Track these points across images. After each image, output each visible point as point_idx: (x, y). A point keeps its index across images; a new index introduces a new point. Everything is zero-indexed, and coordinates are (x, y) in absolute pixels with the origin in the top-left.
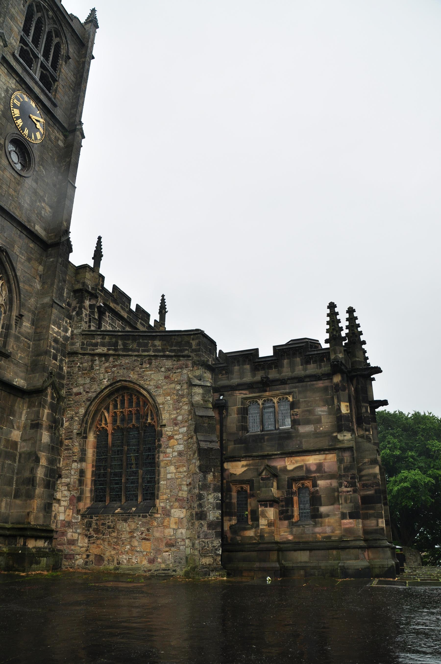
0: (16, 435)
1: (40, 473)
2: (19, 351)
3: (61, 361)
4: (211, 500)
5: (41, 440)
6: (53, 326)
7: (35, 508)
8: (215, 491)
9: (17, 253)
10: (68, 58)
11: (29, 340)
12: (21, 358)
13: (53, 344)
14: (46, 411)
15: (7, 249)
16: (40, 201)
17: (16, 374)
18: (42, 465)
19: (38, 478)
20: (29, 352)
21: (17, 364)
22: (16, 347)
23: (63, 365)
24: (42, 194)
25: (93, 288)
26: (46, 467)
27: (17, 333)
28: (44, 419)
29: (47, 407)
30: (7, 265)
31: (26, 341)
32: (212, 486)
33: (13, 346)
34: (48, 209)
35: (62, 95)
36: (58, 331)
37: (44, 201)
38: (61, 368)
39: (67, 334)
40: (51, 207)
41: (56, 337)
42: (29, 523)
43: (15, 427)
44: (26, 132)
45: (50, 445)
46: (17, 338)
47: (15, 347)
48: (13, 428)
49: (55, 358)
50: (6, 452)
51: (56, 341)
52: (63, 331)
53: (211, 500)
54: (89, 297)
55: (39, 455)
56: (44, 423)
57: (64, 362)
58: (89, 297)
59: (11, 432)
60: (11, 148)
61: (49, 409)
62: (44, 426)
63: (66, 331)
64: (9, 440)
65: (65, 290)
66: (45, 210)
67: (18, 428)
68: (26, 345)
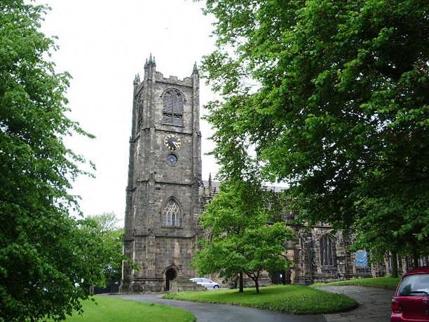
0: (190, 251)
10: (185, 101)
35: (187, 119)
60: (171, 156)
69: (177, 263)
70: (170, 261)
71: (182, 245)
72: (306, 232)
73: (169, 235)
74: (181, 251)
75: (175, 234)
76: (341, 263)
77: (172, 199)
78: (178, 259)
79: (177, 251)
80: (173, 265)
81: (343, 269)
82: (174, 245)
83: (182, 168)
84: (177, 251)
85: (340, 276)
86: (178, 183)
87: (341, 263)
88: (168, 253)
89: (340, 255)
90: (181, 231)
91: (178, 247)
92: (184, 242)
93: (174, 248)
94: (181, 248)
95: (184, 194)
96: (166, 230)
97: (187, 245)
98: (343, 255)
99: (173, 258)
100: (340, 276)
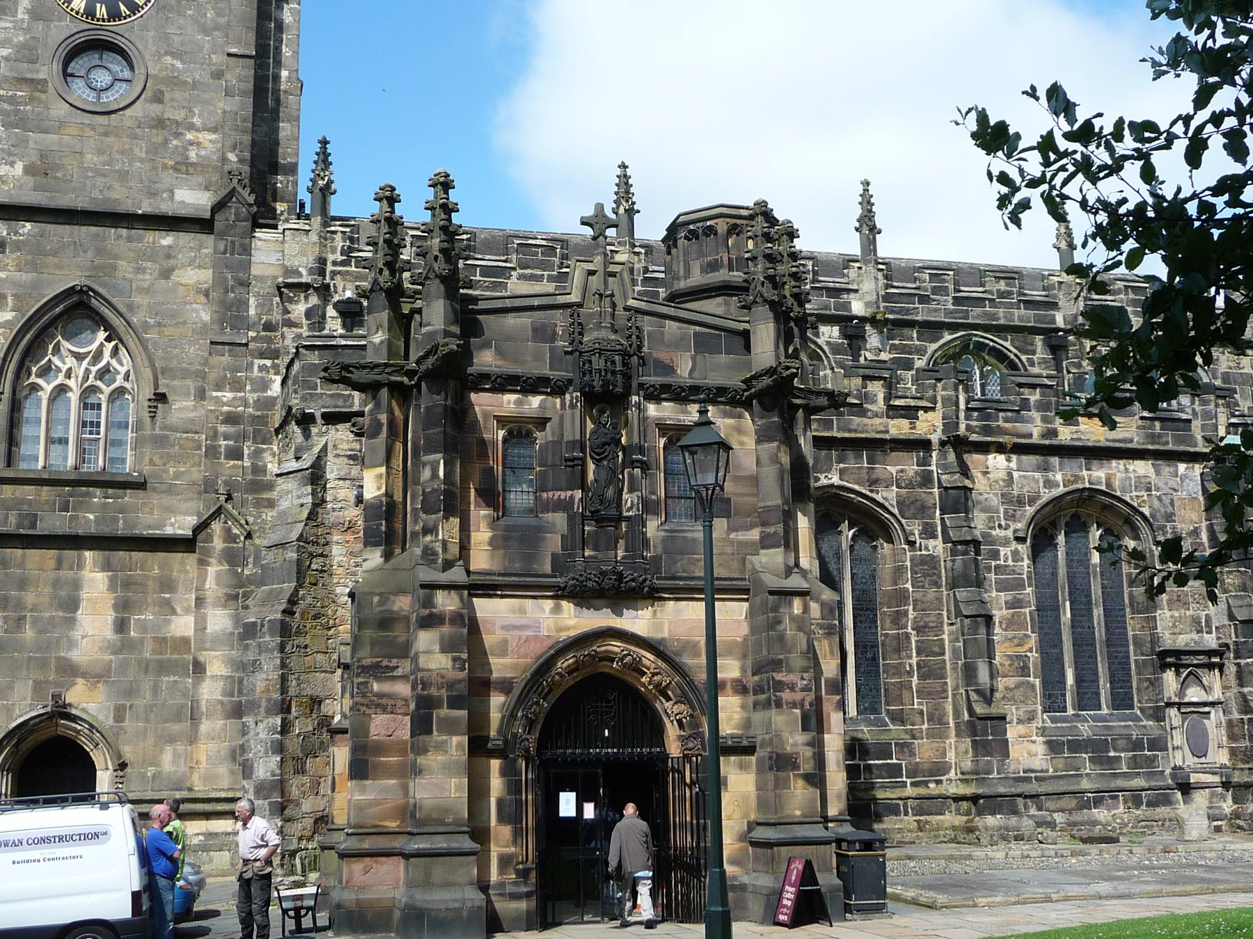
1: (210, 691)
2: (172, 463)
3: (257, 454)
4: (263, 736)
5: (205, 629)
6: (215, 394)
7: (203, 759)
8: (269, 712)
9: (128, 276)
11: (197, 433)
12: (177, 476)
13: (222, 428)
14: (212, 571)
15: (88, 283)
16: (178, 135)
17: (170, 510)
18: (212, 676)
19: (203, 703)
20: (200, 455)
21: (170, 490)
22: (161, 458)
23: (261, 459)
24: (179, 115)
25: (311, 271)
26: (227, 677)
27: (158, 432)
28: (207, 586)
29: (213, 561)
30: (106, 311)
31: (187, 438)
32: (264, 704)
33: (151, 460)
34: (206, 137)
36: (234, 398)
37: (191, 127)
38: (259, 470)
39: (269, 393)
40: (214, 130)
41: (230, 413)
42: (190, 789)
43: (179, 611)
44: (101, 11)
45: (232, 634)
46: (160, 441)
47: (157, 460)
48: (174, 612)
49: (236, 454)
50: (160, 662)
51: (231, 419)
52: (253, 391)
53: (263, 736)
54: (302, 295)
55: (201, 659)
56: (209, 593)
57: (267, 457)
58: (302, 295)
59: (169, 621)
61: (220, 562)
62: (208, 601)
63: (265, 385)
64: (165, 639)
65: (252, 301)
66: (199, 144)
67: (187, 611)
68: (190, 444)
69: (87, 701)
70: (38, 688)
71: (127, 584)
72: (926, 480)
73: (42, 528)
74: (121, 626)
75: (89, 520)
76: (1194, 694)
77: (77, 310)
78: (96, 676)
79: (94, 626)
80: (61, 712)
81: (1214, 724)
82: (77, 585)
83: (160, 123)
84: (94, 626)
85: (1186, 788)
86: (127, 206)
87: (1194, 694)
88: (29, 633)
89: (1184, 640)
90: (129, 497)
91: (109, 600)
92: (155, 563)
93: (72, 605)
94: (124, 608)
95: (166, 274)
96: (28, 492)
97: (167, 585)
98: (1211, 641)
99: (70, 671)
100: (1186, 788)
